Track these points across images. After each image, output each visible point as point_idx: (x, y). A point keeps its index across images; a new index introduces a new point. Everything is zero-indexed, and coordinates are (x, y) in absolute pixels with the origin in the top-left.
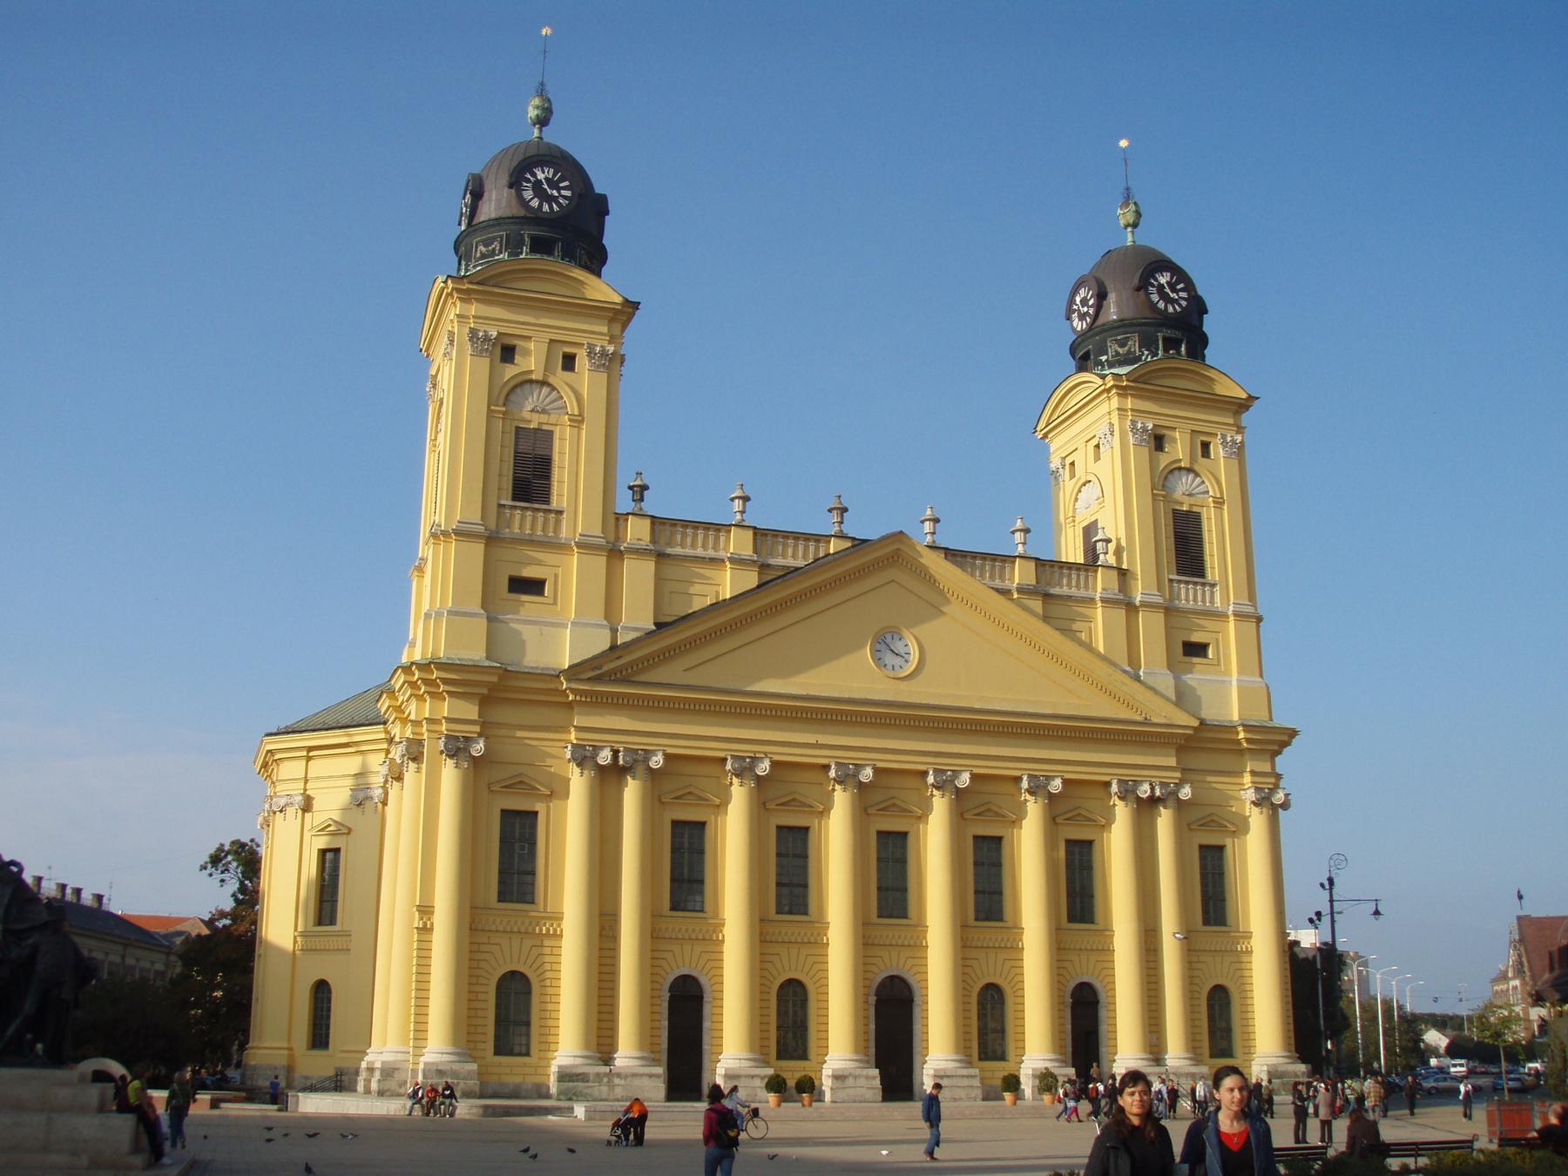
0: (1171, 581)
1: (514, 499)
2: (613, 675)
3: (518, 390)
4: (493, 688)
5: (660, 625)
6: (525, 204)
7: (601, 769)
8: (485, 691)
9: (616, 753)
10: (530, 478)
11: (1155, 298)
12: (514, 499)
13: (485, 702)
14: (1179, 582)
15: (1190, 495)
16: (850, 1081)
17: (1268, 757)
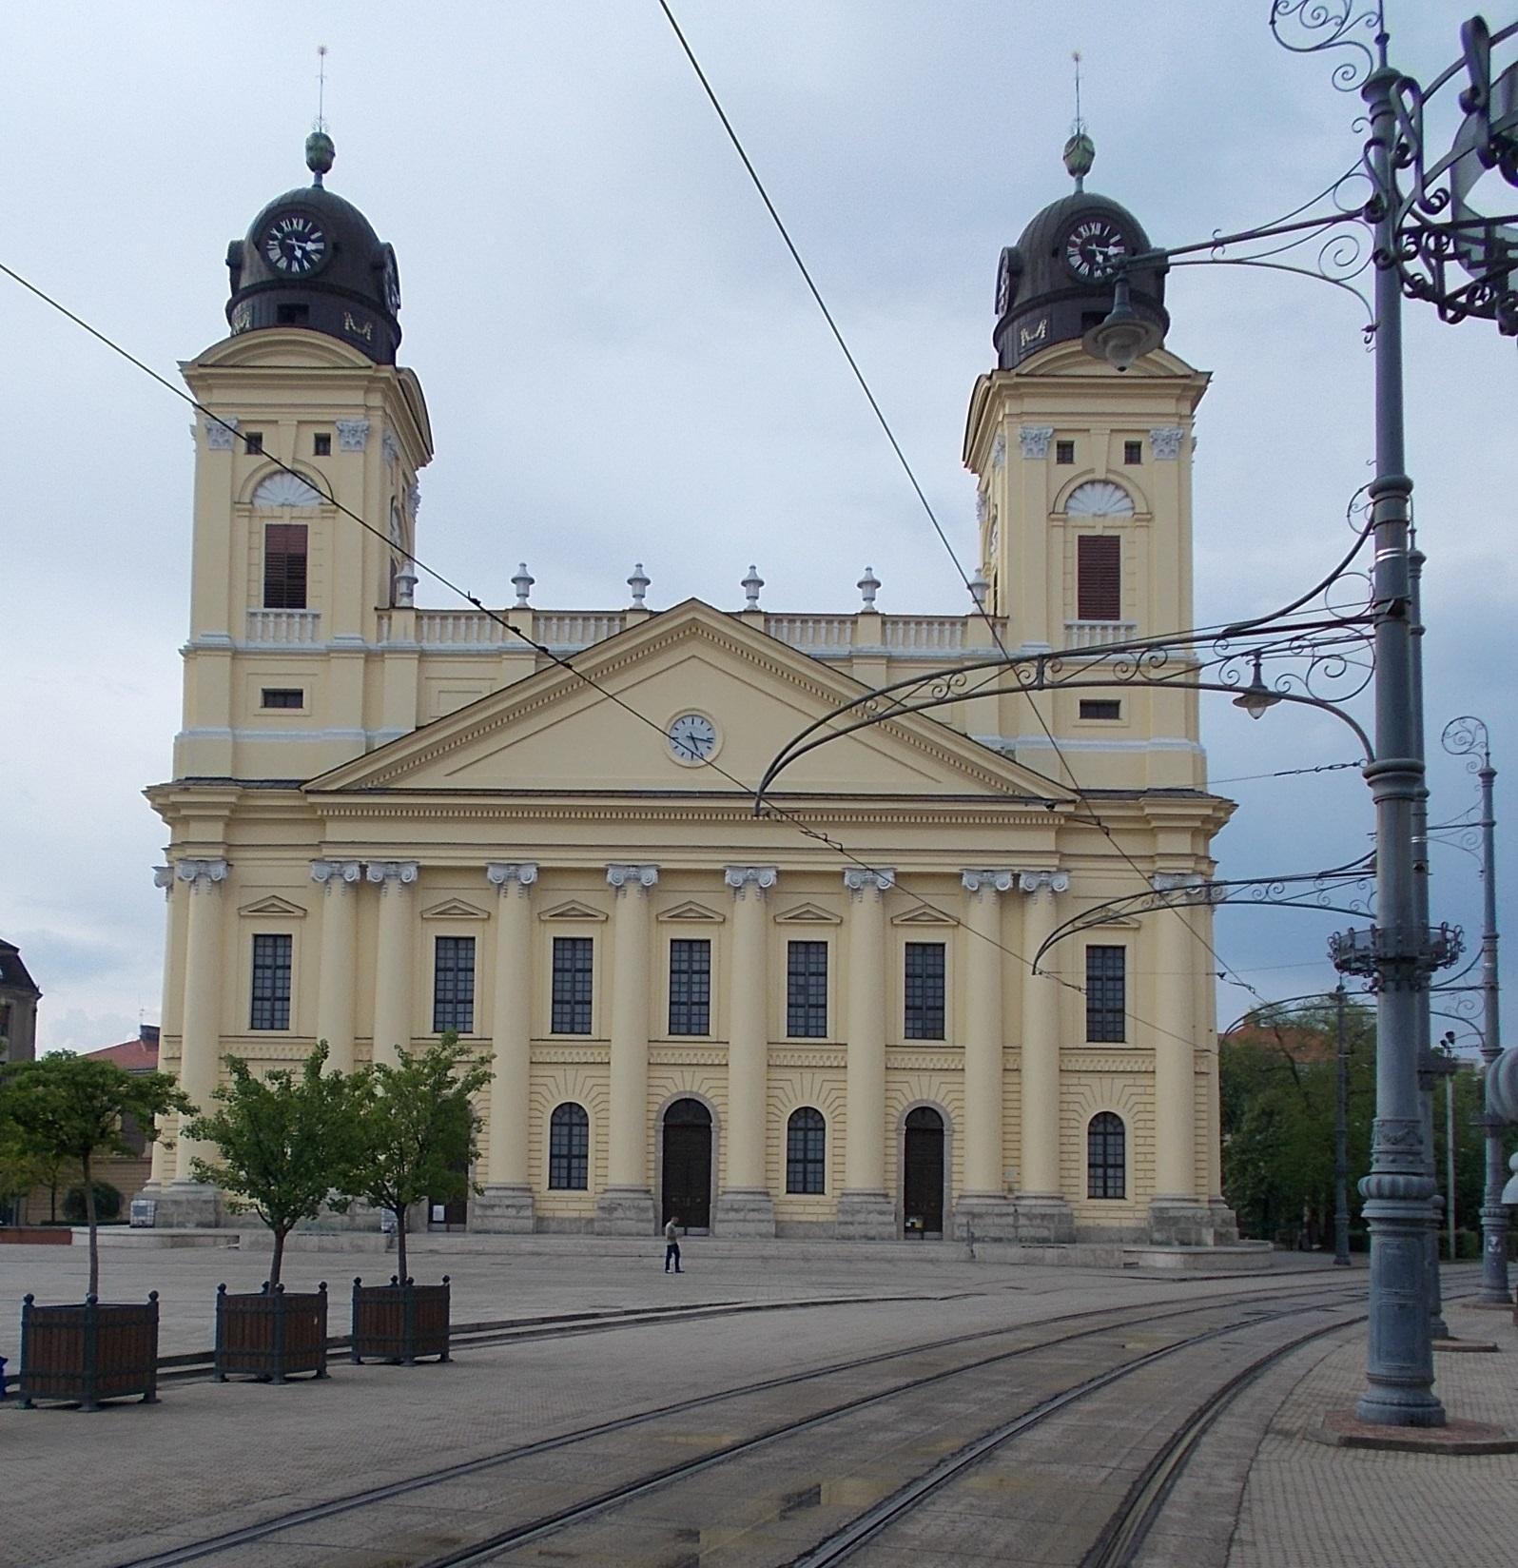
0: (1068, 627)
1: (267, 605)
2: (373, 786)
3: (267, 483)
4: (235, 808)
5: (418, 729)
6: (272, 266)
7: (353, 885)
8: (226, 813)
9: (363, 869)
10: (286, 582)
11: (1076, 261)
12: (267, 605)
13: (230, 823)
14: (1081, 627)
15: (1104, 515)
16: (619, 1213)
17: (1187, 838)
